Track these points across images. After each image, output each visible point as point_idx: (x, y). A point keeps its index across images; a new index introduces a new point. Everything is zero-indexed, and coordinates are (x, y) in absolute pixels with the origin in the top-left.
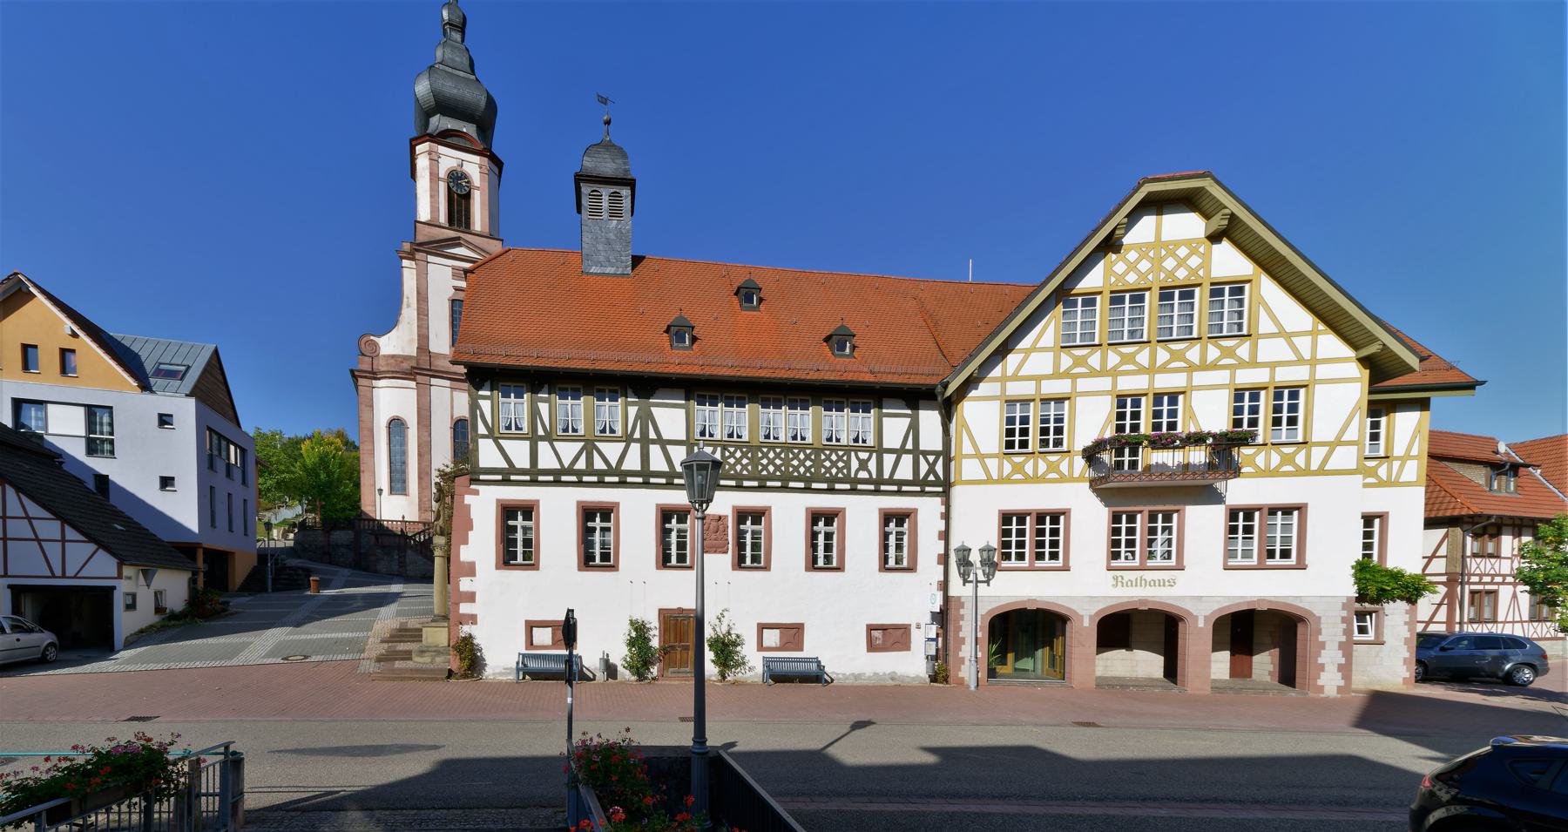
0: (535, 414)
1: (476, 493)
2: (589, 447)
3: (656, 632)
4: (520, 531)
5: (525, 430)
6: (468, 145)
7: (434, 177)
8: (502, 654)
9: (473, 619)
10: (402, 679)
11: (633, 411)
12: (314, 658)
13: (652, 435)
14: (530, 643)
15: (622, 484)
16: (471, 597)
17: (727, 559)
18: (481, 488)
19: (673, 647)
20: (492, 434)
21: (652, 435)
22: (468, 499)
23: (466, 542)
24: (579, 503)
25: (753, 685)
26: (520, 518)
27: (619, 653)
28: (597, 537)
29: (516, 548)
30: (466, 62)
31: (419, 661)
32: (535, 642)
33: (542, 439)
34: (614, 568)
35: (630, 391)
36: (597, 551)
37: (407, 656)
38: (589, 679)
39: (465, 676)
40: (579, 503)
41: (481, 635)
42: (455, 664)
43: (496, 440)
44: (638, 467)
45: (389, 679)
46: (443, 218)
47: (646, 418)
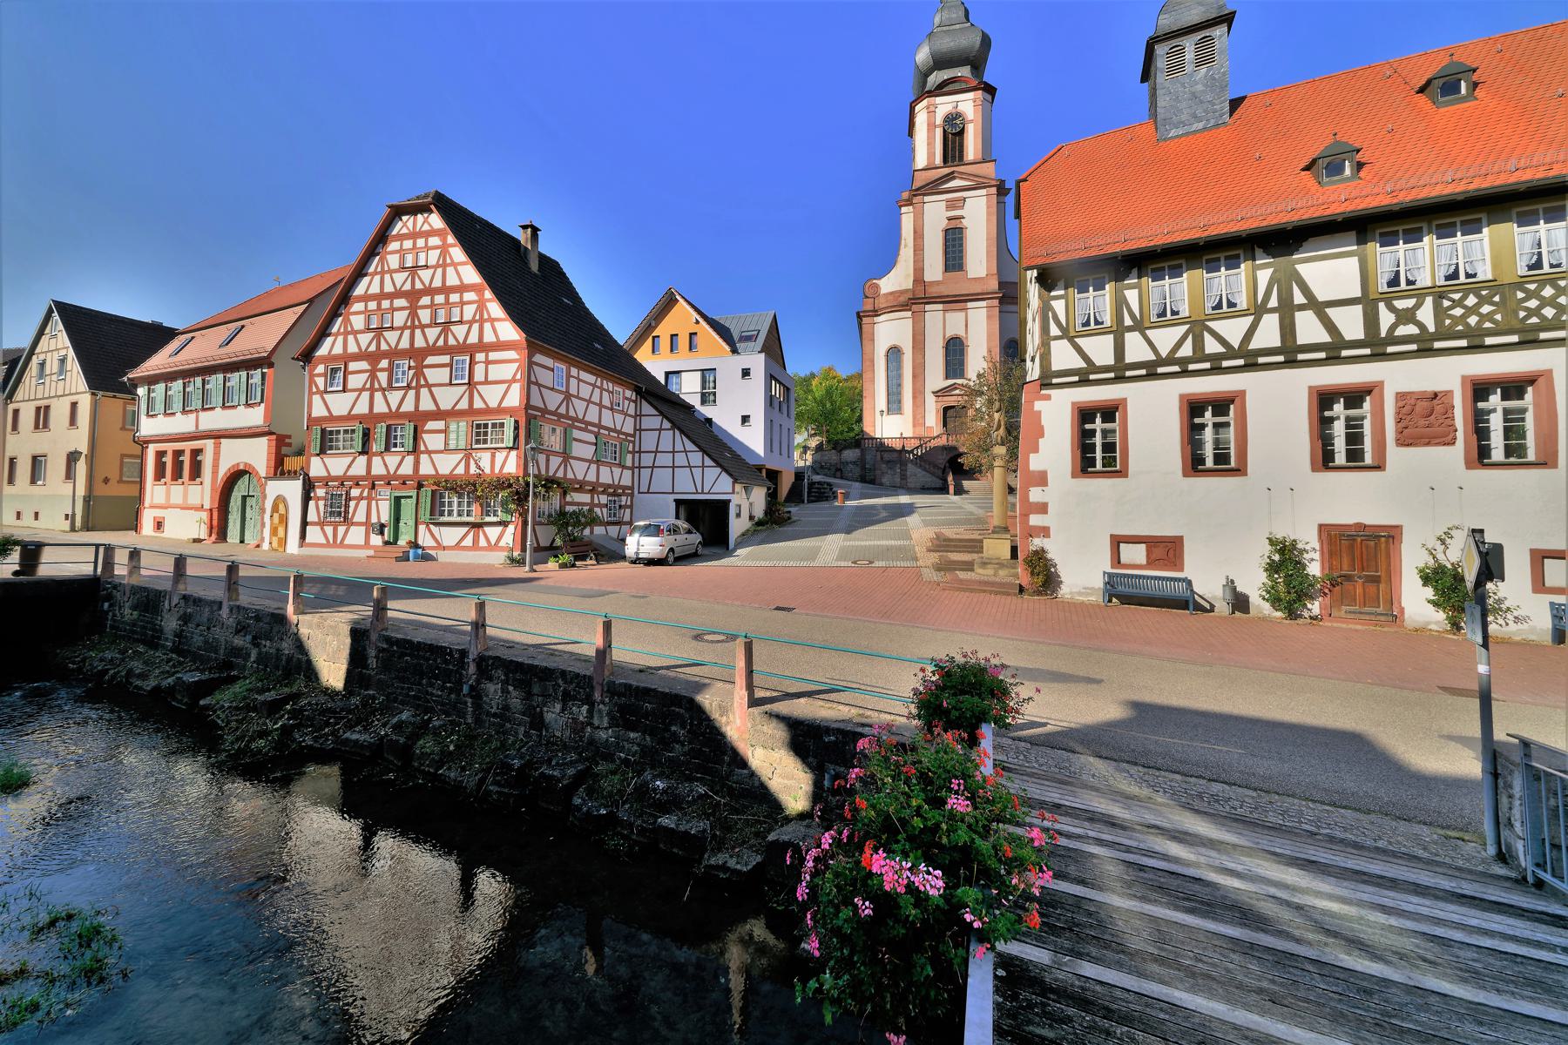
0: (1120, 303)
1: (1048, 398)
2: (1197, 328)
3: (1317, 556)
4: (1098, 434)
5: (1108, 323)
6: (964, 86)
7: (931, 126)
8: (1082, 574)
9: (1045, 532)
10: (972, 591)
11: (1264, 276)
12: (877, 564)
13: (1299, 298)
14: (1116, 560)
15: (1251, 366)
16: (1042, 508)
17: (1456, 453)
18: (1053, 393)
19: (1348, 578)
20: (1066, 334)
21: (1299, 298)
22: (1038, 405)
23: (1036, 450)
24: (1182, 397)
25: (1526, 645)
26: (1098, 420)
27: (1254, 583)
28: (1208, 434)
29: (1098, 448)
30: (962, 13)
31: (980, 573)
32: (1123, 559)
33: (1130, 329)
34: (1240, 471)
35: (1259, 252)
36: (1209, 452)
37: (969, 566)
38: (1204, 610)
39: (1039, 593)
40: (1182, 397)
41: (1054, 549)
42: (1022, 575)
43: (1071, 340)
44: (1275, 342)
45: (959, 589)
46: (938, 160)
47: (1286, 281)
